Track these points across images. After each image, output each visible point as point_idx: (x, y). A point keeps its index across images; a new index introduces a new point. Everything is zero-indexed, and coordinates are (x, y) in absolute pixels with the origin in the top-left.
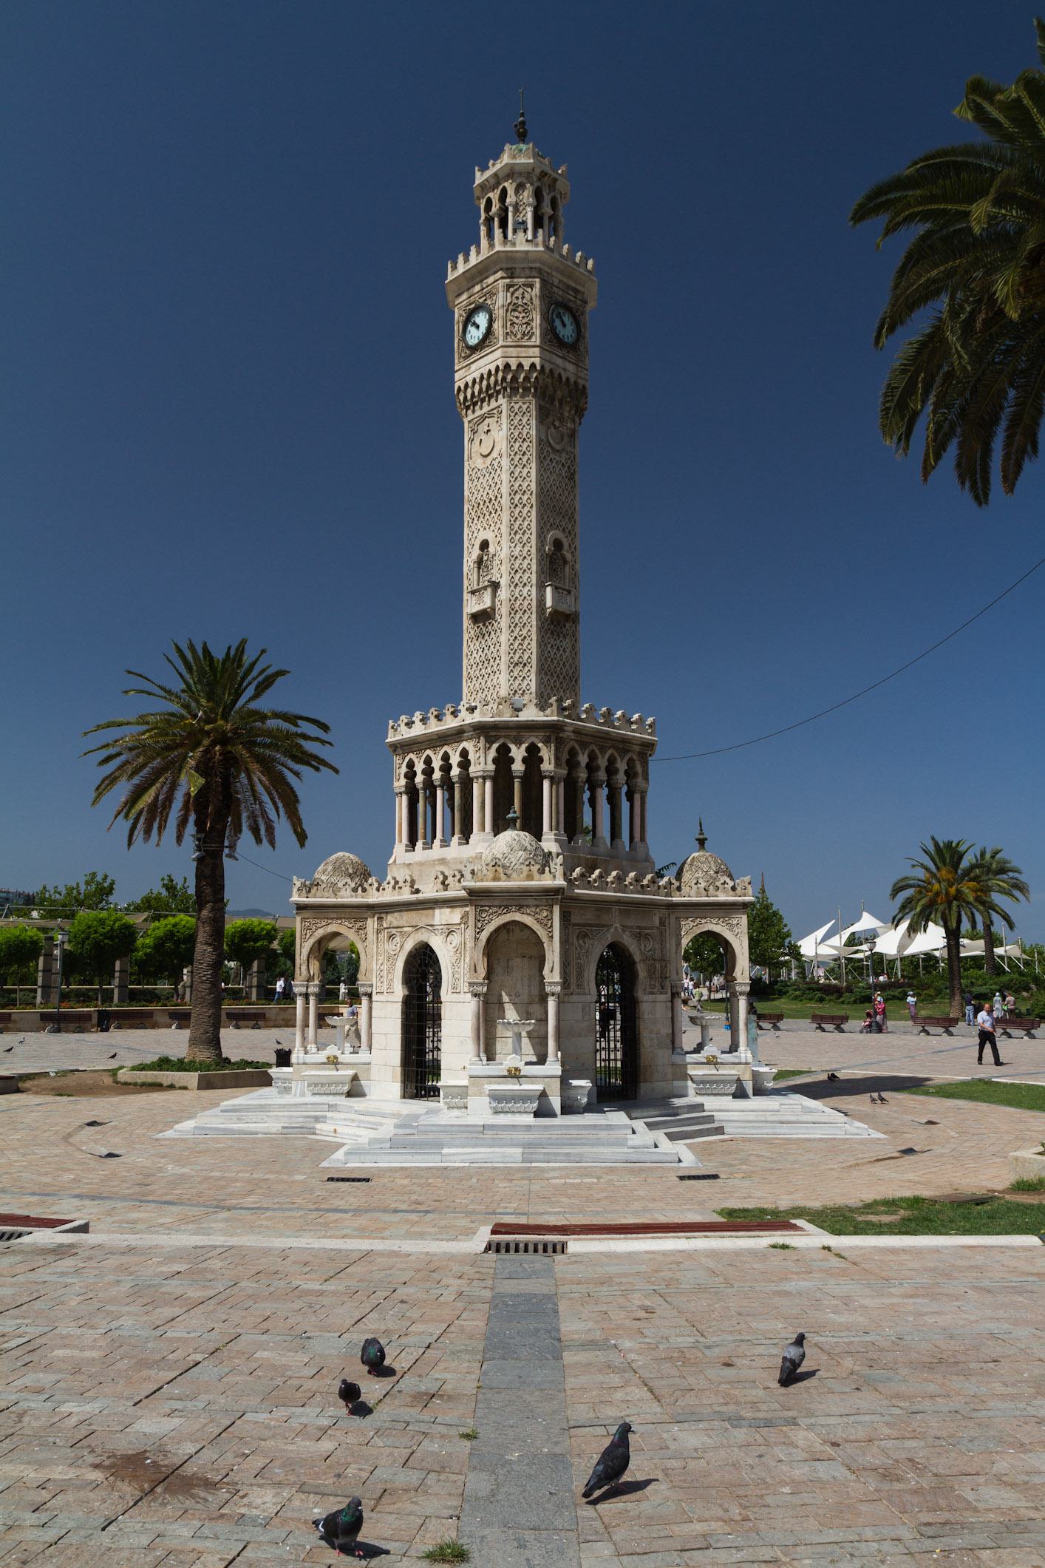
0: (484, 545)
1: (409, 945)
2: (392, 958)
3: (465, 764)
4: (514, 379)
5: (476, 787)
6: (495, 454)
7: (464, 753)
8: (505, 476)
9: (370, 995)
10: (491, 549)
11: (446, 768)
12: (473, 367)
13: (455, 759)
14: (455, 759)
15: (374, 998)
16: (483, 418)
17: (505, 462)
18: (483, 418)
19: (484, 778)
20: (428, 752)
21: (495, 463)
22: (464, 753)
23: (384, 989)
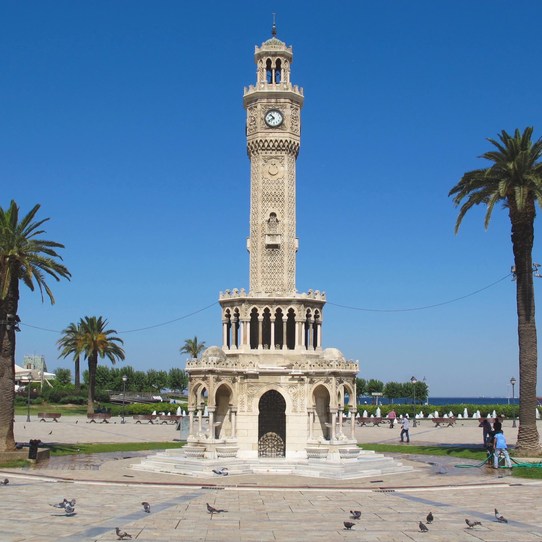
0: (273, 215)
1: (264, 390)
2: (251, 396)
3: (291, 313)
4: (291, 147)
5: (297, 325)
6: (279, 176)
7: (291, 311)
8: (286, 189)
9: (236, 412)
10: (278, 217)
11: (279, 313)
12: (271, 135)
13: (285, 312)
14: (285, 312)
15: (238, 414)
16: (272, 158)
17: (286, 182)
18: (272, 158)
19: (302, 322)
20: (267, 306)
21: (281, 181)
22: (291, 311)
23: (246, 408)
